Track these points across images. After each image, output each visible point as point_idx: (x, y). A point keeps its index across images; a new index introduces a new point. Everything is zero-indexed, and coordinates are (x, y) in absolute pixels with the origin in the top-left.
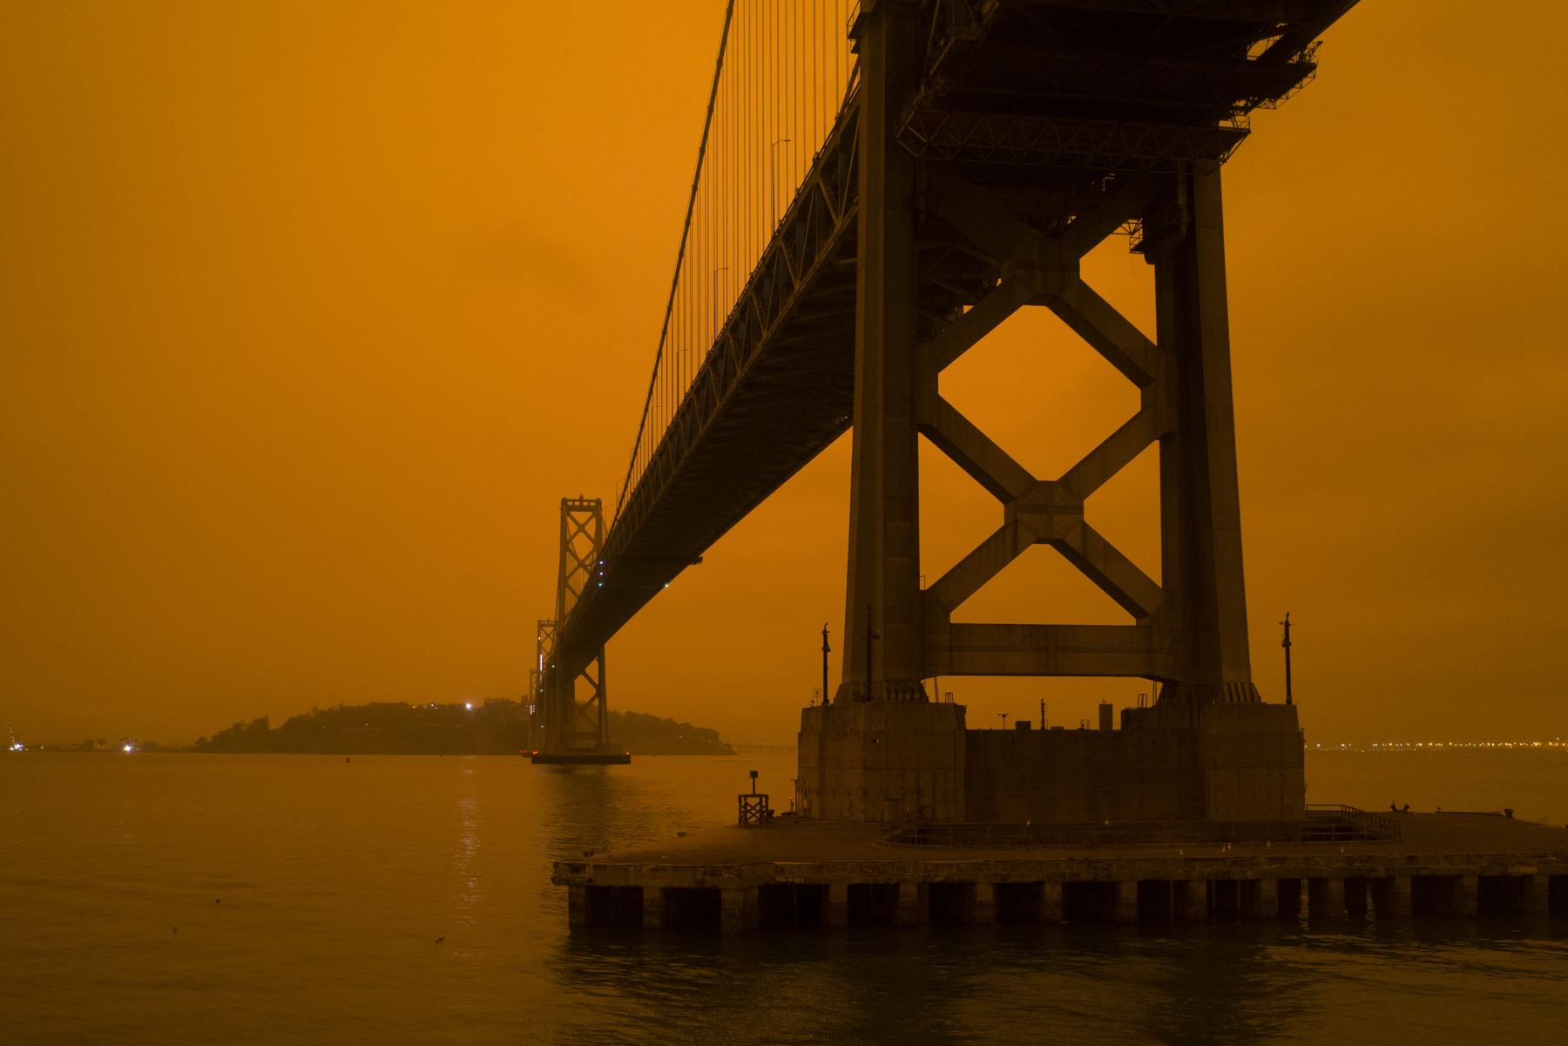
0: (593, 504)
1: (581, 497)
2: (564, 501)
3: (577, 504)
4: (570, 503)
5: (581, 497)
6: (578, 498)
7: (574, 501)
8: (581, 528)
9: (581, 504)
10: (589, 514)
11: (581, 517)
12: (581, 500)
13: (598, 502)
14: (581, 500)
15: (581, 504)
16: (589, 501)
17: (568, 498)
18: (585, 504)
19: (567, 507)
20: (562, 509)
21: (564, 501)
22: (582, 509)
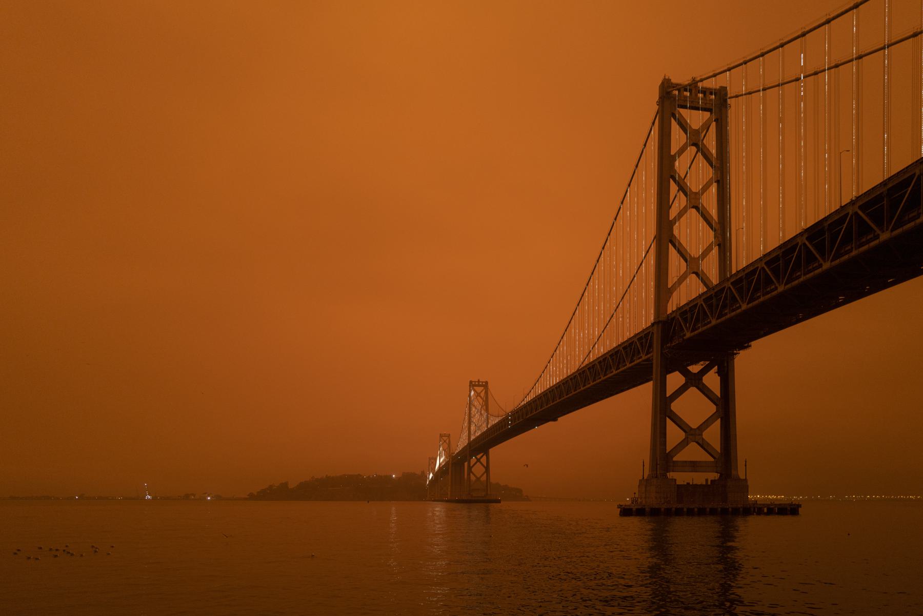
0: (484, 383)
1: (479, 380)
2: (471, 382)
3: (477, 383)
4: (473, 383)
5: (479, 380)
6: (477, 381)
7: (475, 382)
10: (483, 388)
12: (479, 381)
13: (487, 383)
14: (479, 381)
16: (482, 382)
17: (473, 380)
18: (481, 383)
21: (471, 382)
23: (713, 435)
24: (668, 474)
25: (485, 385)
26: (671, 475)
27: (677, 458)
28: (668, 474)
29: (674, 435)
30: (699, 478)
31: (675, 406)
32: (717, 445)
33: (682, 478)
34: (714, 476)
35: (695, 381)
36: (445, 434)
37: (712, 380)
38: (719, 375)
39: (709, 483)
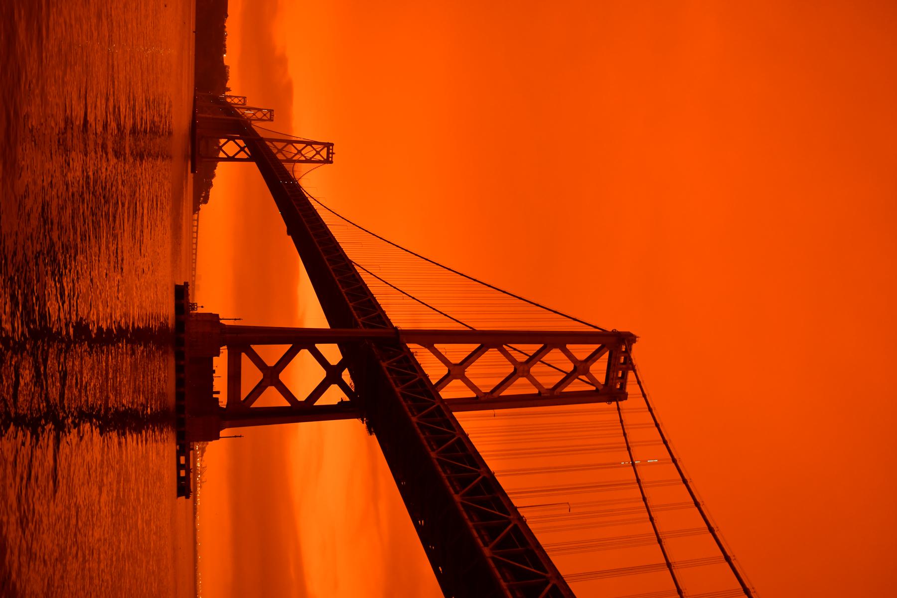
0: (330, 159)
1: (334, 153)
3: (331, 151)
4: (331, 147)
5: (334, 153)
7: (332, 149)
8: (318, 153)
9: (331, 153)
10: (325, 157)
11: (324, 153)
12: (333, 153)
13: (331, 162)
14: (333, 153)
15: (331, 153)
16: (332, 157)
17: (334, 146)
18: (331, 155)
19: (329, 146)
20: (328, 143)
21: (332, 145)
22: (328, 153)
23: (272, 398)
24: (225, 347)
25: (328, 161)
26: (224, 350)
27: (245, 358)
28: (225, 347)
29: (272, 353)
30: (220, 384)
31: (305, 355)
32: (260, 403)
33: (221, 363)
34: (223, 400)
35: (333, 375)
36: (273, 116)
37: (334, 396)
38: (339, 403)
39: (215, 396)
